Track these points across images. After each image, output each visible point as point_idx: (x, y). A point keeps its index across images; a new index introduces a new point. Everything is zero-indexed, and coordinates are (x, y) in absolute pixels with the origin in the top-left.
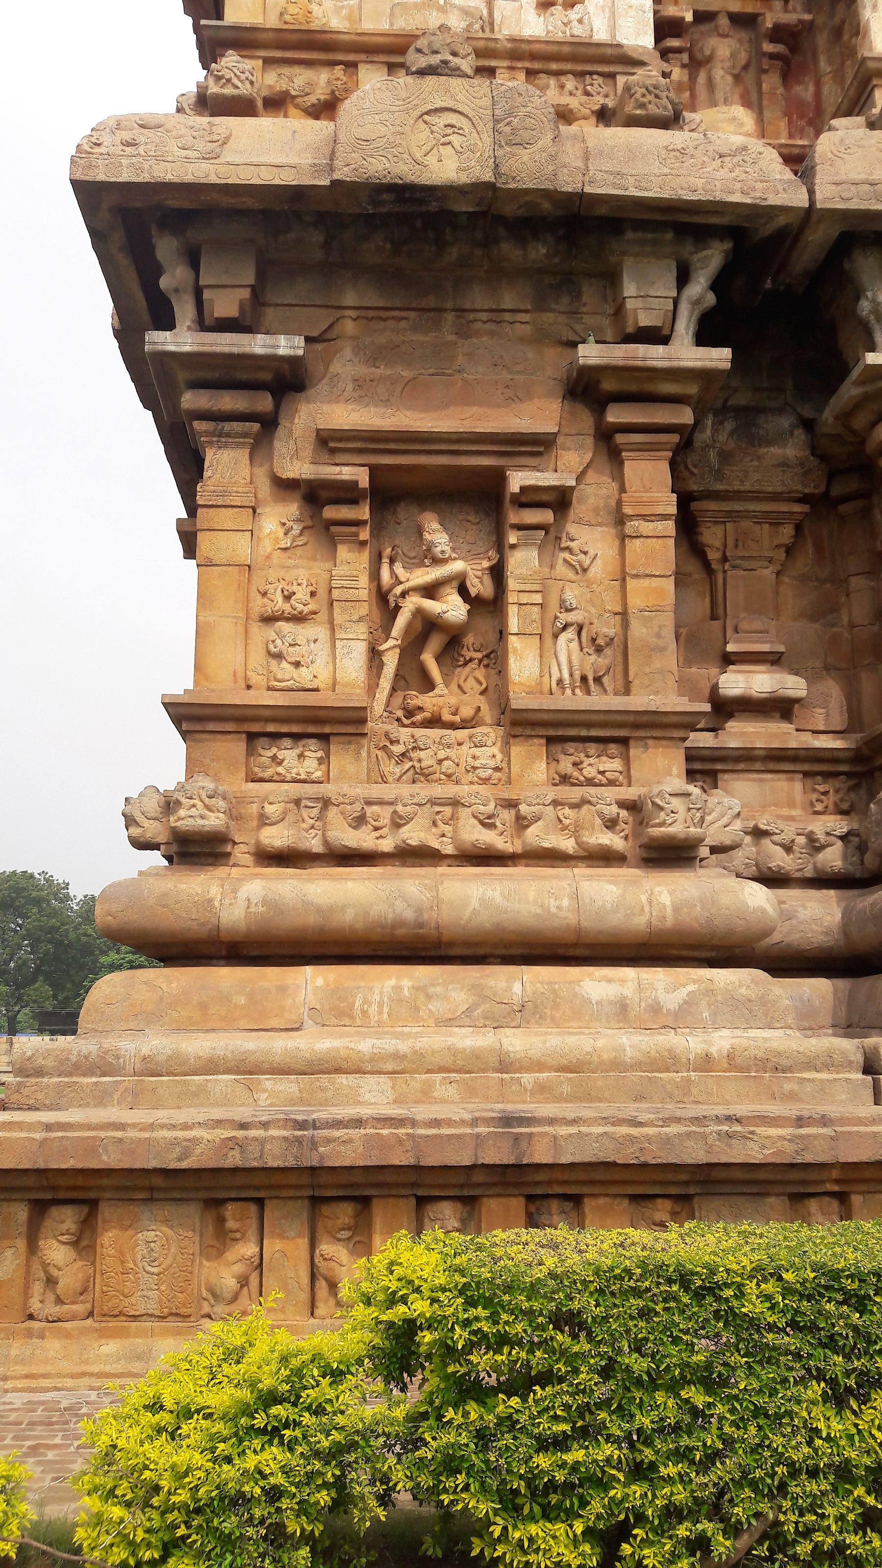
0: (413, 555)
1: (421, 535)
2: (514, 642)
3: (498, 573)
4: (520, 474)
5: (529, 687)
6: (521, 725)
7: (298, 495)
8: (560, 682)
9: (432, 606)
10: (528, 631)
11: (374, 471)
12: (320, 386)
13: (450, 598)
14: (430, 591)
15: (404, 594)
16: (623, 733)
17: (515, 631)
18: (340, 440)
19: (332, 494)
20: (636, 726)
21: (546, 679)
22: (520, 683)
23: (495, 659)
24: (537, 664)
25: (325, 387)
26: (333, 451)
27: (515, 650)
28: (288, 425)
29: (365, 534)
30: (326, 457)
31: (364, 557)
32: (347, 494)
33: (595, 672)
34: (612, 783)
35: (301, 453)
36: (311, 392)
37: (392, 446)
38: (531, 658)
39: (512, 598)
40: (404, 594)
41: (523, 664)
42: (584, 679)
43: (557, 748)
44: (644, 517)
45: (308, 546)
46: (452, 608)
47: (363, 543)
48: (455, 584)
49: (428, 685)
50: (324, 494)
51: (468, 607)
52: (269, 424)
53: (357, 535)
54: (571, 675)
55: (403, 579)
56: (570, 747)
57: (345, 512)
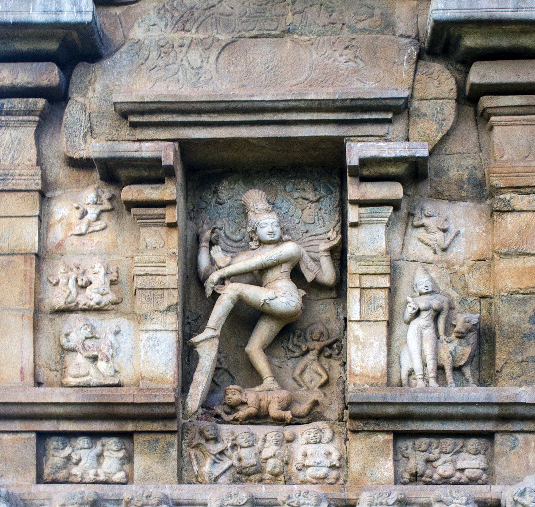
0: (238, 237)
1: (245, 214)
2: (355, 330)
3: (339, 254)
4: (359, 144)
5: (374, 378)
6: (364, 417)
7: (96, 175)
8: (411, 373)
9: (256, 294)
10: (372, 317)
11: (185, 147)
12: (118, 55)
13: (279, 284)
14: (257, 276)
15: (222, 281)
16: (488, 427)
17: (357, 318)
18: (142, 113)
19: (133, 173)
20: (503, 419)
21: (395, 370)
22: (362, 375)
23: (334, 347)
24: (384, 354)
25: (124, 56)
26: (134, 125)
27: (357, 338)
28: (80, 99)
29: (171, 215)
30: (126, 132)
31: (173, 241)
32: (152, 172)
33: (454, 360)
34: (472, 481)
35: (96, 130)
36: (107, 63)
37: (205, 118)
38: (376, 347)
39: (352, 281)
40: (222, 281)
41: (365, 354)
42: (440, 369)
43: (406, 445)
44: (517, 189)
45: (106, 232)
46: (281, 295)
47: (172, 226)
48: (286, 268)
49: (256, 378)
50: (123, 173)
51: (303, 293)
52: (57, 98)
53: (162, 217)
54: (425, 365)
55: (221, 264)
56: (423, 442)
57: (149, 193)
